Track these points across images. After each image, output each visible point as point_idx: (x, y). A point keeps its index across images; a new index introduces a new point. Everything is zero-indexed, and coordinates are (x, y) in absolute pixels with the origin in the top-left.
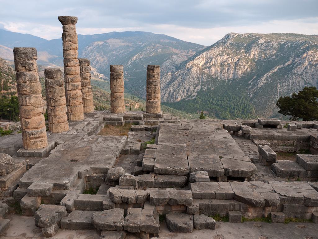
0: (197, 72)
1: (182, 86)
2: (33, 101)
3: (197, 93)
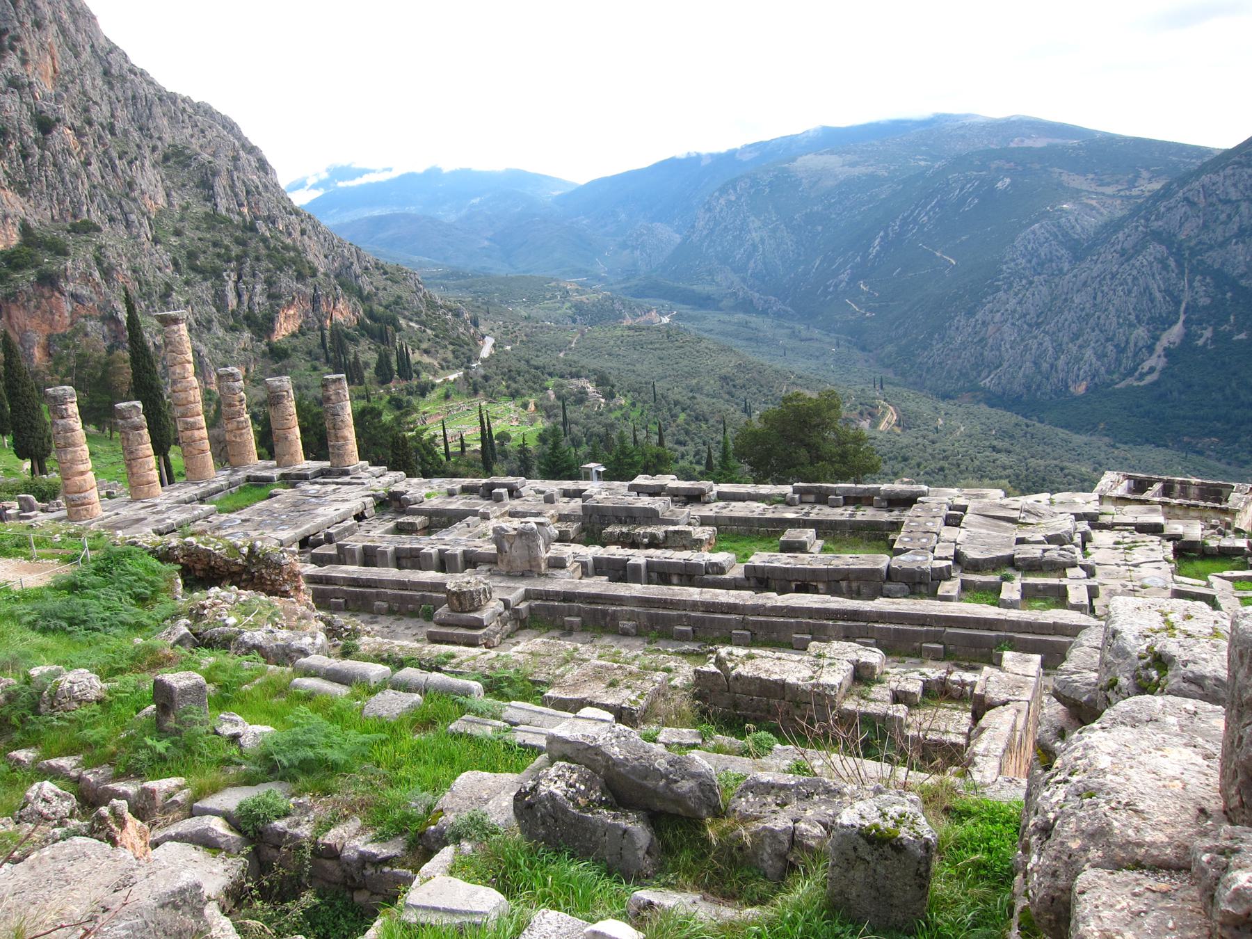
0: (1165, 267)
1: (1097, 332)
2: (69, 457)
3: (1166, 356)
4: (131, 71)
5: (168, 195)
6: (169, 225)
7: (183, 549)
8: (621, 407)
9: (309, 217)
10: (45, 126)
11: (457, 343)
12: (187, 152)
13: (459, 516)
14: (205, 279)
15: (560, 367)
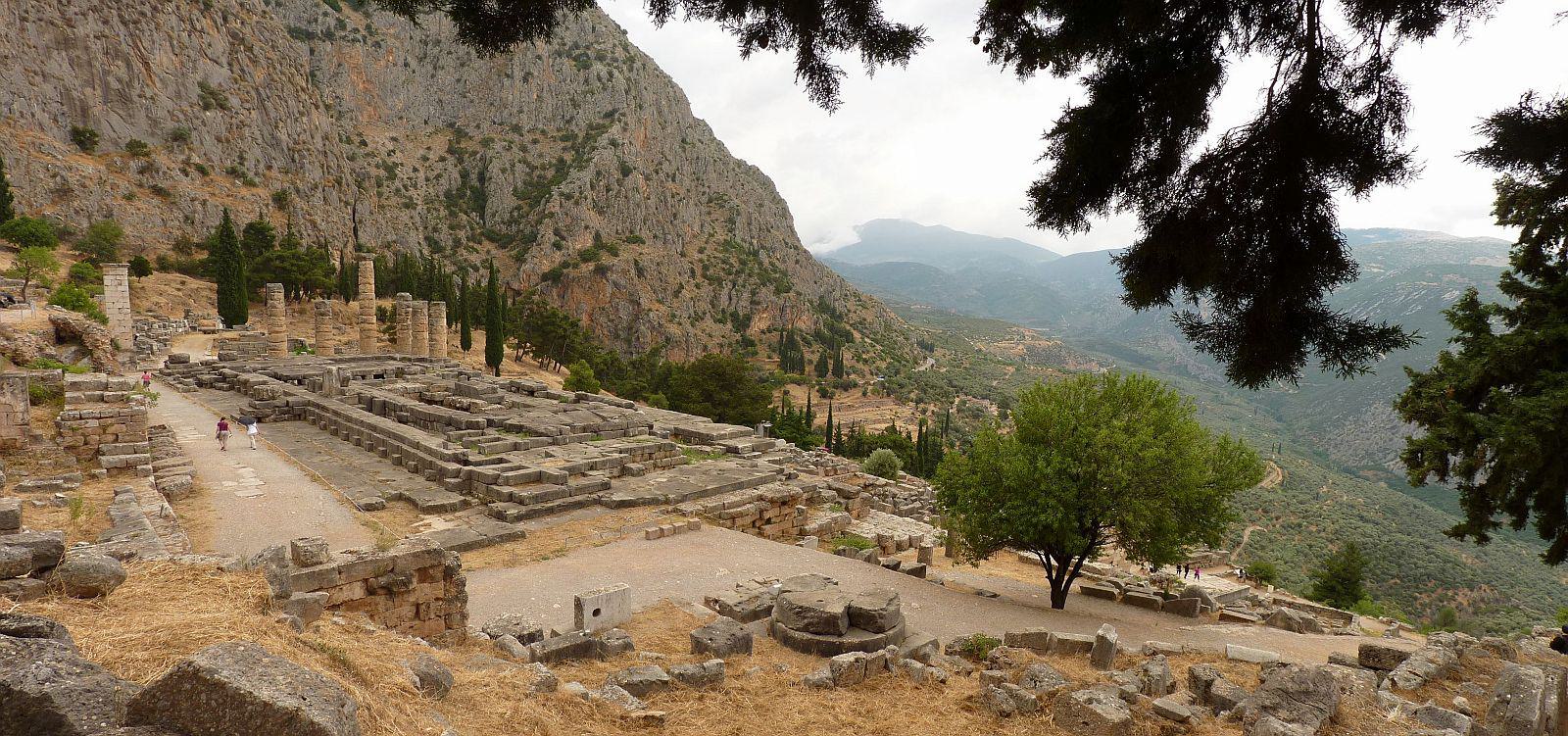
4: (699, 140)
6: (699, 243)
10: (626, 171)
12: (725, 197)
14: (710, 285)
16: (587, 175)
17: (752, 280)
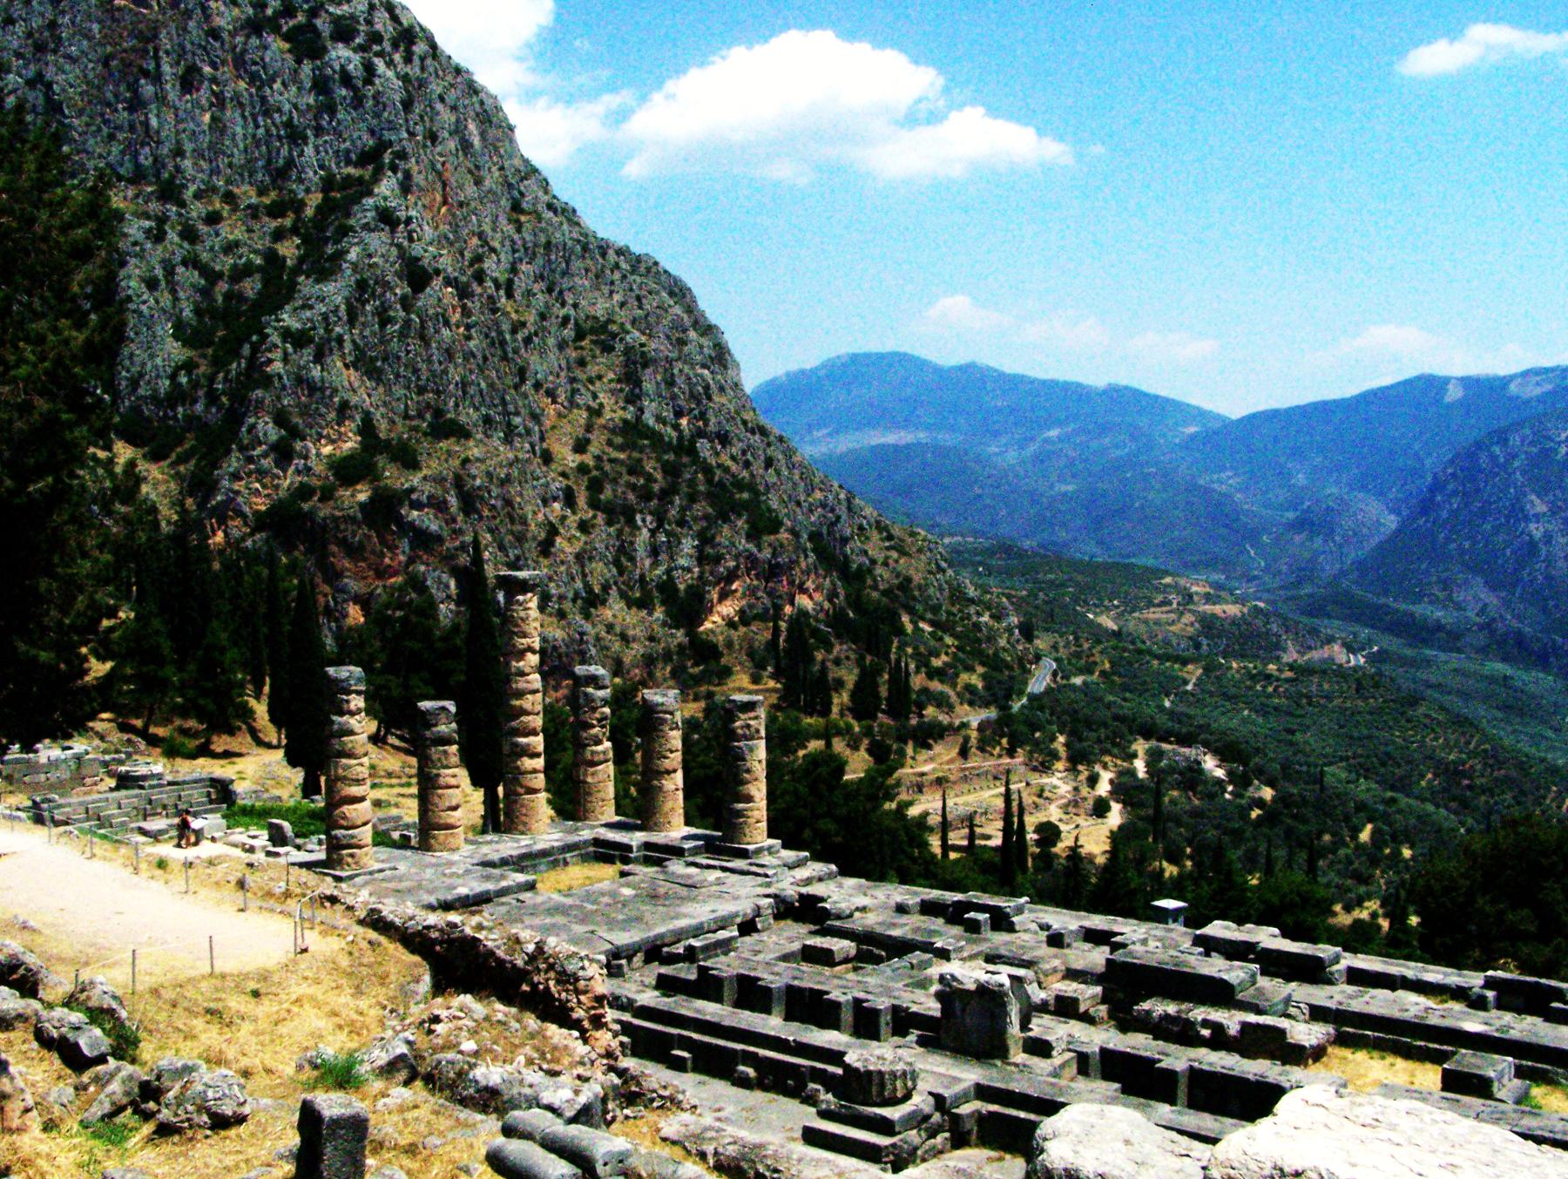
4: (550, 207)
5: (574, 392)
7: (441, 930)
8: (1260, 803)
9: (781, 439)
11: (994, 664)
12: (614, 328)
13: (900, 948)
14: (609, 523)
15: (1162, 720)
16: (336, 291)
17: (701, 508)
